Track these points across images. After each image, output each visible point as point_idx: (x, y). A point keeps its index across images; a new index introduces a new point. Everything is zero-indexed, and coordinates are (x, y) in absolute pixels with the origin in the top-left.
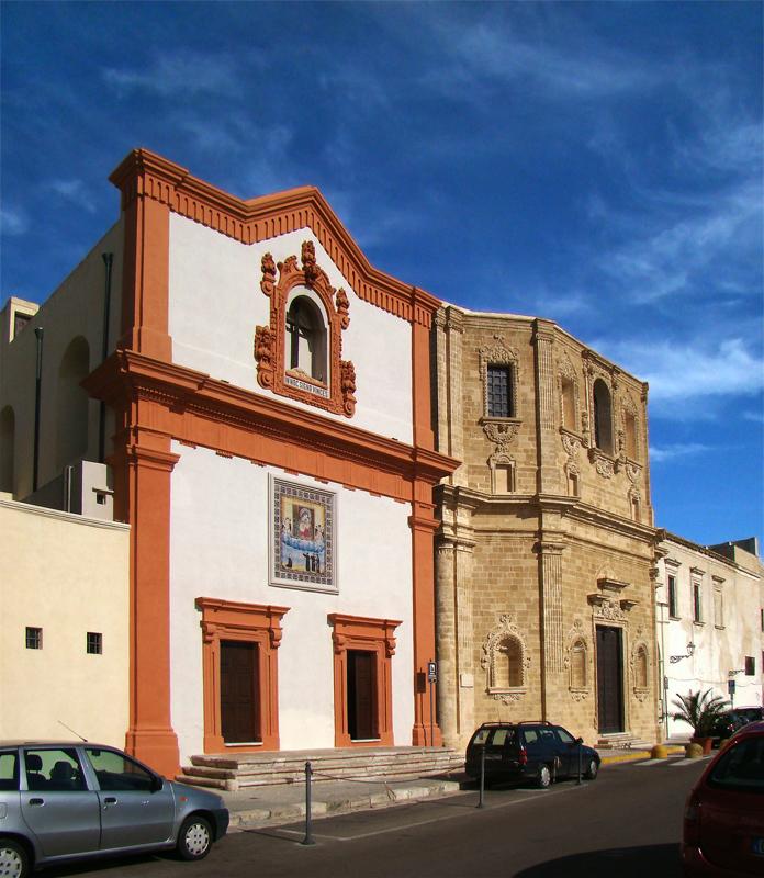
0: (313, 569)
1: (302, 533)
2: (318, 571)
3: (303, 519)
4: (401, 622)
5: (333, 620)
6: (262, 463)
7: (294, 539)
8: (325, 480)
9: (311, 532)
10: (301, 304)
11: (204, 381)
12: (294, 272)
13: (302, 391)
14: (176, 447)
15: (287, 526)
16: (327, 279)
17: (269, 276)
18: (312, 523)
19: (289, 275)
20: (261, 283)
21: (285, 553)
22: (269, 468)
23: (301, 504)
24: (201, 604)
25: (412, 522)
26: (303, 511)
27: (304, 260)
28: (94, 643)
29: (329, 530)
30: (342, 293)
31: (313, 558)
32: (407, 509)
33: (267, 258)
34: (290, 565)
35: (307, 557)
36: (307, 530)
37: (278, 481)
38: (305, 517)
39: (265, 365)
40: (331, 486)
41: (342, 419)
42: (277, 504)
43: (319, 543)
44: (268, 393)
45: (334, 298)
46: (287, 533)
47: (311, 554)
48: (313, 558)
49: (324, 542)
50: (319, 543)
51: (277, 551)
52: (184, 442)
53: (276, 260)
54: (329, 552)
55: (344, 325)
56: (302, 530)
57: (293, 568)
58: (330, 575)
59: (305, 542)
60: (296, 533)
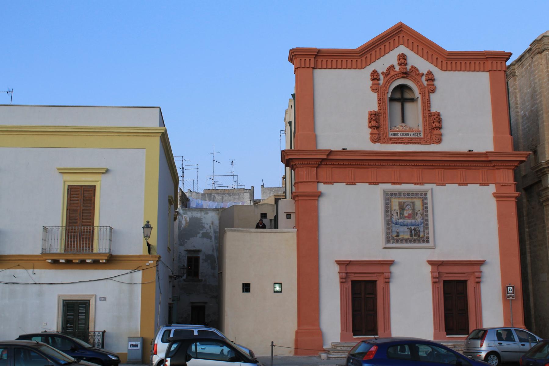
0: (415, 236)
1: (406, 217)
2: (419, 236)
3: (406, 209)
5: (431, 263)
6: (376, 183)
7: (400, 221)
8: (422, 184)
9: (413, 215)
10: (402, 88)
11: (331, 152)
12: (392, 73)
13: (403, 138)
14: (322, 187)
15: (395, 215)
16: (417, 69)
17: (376, 82)
18: (414, 209)
19: (389, 76)
20: (371, 87)
21: (394, 229)
24: (339, 263)
25: (497, 196)
26: (406, 204)
27: (400, 65)
28: (246, 288)
29: (427, 212)
30: (430, 73)
31: (415, 230)
32: (492, 188)
33: (375, 73)
34: (398, 236)
36: (409, 214)
37: (385, 191)
38: (408, 207)
39: (376, 131)
40: (427, 186)
43: (419, 219)
45: (424, 78)
46: (395, 218)
48: (415, 230)
49: (423, 219)
50: (419, 219)
52: (325, 183)
53: (380, 72)
54: (427, 225)
55: (433, 91)
56: (406, 214)
57: (400, 237)
58: (428, 237)
59: (408, 221)
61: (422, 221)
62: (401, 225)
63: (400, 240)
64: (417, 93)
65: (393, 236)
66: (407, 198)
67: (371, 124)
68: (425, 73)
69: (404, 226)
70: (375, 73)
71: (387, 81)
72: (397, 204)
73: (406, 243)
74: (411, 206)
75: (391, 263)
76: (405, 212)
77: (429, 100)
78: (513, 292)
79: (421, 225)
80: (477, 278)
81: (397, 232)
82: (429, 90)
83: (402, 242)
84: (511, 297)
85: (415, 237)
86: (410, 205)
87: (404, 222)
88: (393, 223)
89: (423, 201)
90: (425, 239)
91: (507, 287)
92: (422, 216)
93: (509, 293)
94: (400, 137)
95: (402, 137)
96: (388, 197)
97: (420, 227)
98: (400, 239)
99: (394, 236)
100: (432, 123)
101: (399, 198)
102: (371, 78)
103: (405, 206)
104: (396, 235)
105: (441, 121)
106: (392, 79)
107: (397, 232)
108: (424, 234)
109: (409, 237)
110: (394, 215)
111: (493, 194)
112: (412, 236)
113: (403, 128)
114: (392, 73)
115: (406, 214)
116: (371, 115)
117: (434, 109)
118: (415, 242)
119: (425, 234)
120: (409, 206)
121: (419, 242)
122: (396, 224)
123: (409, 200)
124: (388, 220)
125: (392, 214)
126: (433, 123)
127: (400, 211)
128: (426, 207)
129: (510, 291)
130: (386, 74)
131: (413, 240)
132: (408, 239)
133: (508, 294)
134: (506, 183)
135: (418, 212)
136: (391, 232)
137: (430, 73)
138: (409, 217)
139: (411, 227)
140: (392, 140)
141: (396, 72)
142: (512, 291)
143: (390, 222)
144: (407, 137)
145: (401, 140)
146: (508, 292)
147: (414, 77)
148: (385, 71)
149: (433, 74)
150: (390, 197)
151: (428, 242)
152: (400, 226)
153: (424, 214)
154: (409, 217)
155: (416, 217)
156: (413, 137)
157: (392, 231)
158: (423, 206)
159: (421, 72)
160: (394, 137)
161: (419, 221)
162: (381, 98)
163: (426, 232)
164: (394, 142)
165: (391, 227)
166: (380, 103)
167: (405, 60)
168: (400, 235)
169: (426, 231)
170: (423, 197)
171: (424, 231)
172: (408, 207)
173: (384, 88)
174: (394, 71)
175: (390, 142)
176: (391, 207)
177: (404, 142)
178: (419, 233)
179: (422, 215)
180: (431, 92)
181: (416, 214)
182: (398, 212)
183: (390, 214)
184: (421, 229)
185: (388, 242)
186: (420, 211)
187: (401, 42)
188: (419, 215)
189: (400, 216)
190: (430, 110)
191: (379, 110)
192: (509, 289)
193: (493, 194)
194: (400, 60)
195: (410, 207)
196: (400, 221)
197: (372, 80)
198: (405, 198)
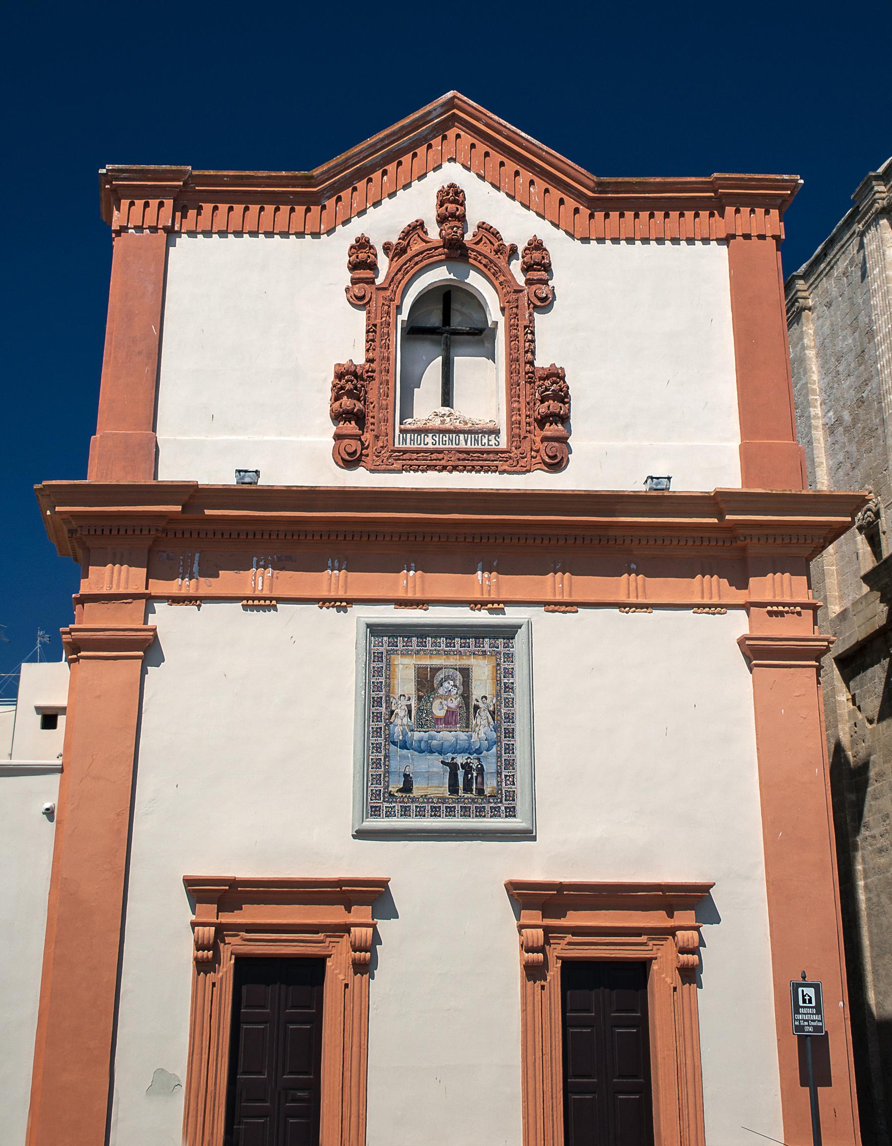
0: (468, 788)
1: (438, 720)
2: (481, 792)
3: (441, 691)
4: (714, 884)
7: (417, 735)
12: (417, 246)
13: (440, 452)
15: (401, 712)
16: (496, 234)
18: (466, 696)
19: (405, 257)
20: (347, 290)
21: (394, 765)
23: (437, 662)
26: (440, 675)
27: (442, 220)
29: (510, 703)
30: (536, 246)
31: (467, 767)
33: (362, 244)
34: (407, 787)
35: (453, 767)
36: (450, 712)
39: (351, 427)
46: (401, 723)
47: (460, 760)
48: (467, 767)
49: (496, 729)
53: (378, 243)
54: (510, 749)
55: (545, 304)
56: (439, 712)
57: (416, 793)
58: (511, 796)
59: (446, 736)
60: (424, 720)
61: (494, 735)
62: (421, 752)
63: (413, 806)
64: (495, 314)
65: (390, 789)
66: (447, 653)
67: (338, 403)
69: (431, 752)
70: (362, 244)
71: (399, 270)
72: (411, 674)
73: (435, 815)
74: (458, 683)
76: (437, 703)
77: (530, 328)
79: (488, 750)
80: (683, 951)
81: (406, 776)
83: (421, 813)
84: (811, 1029)
85: (466, 796)
86: (454, 680)
87: (432, 738)
88: (394, 743)
89: (498, 665)
90: (501, 802)
91: (796, 986)
92: (494, 720)
93: (801, 1010)
94: (430, 446)
95: (437, 446)
96: (381, 649)
98: (414, 800)
100: (538, 403)
101: (418, 652)
102: (350, 262)
105: (567, 395)
106: (416, 264)
107: (406, 776)
108: (498, 782)
109: (447, 794)
110: (397, 714)
111: (741, 642)
112: (458, 793)
113: (443, 422)
114: (417, 246)
116: (339, 376)
117: (542, 361)
119: (501, 782)
120: (452, 683)
121: (480, 813)
122: (404, 746)
123: (453, 661)
125: (392, 712)
126: (542, 402)
127: (419, 698)
128: (509, 688)
129: (804, 1001)
130: (395, 251)
131: (458, 807)
132: (443, 800)
133: (800, 1017)
134: (784, 605)
135: (481, 705)
136: (385, 777)
137: (536, 246)
138: (449, 720)
139: (453, 759)
140: (405, 457)
141: (427, 242)
142: (814, 1004)
143: (381, 740)
144: (454, 446)
145: (434, 456)
146: (797, 1008)
147: (486, 257)
148: (394, 240)
149: (545, 250)
150: (387, 651)
151: (511, 812)
152: (416, 753)
153: (500, 711)
154: (449, 720)
155: (474, 722)
156: (473, 446)
157: (387, 772)
158: (498, 682)
160: (412, 446)
161: (482, 735)
162: (378, 321)
163: (506, 776)
164: (410, 462)
165: (386, 756)
166: (373, 341)
167: (462, 204)
171: (499, 773)
172: (446, 684)
173: (388, 293)
174: (427, 242)
175: (397, 465)
176: (388, 685)
177: (443, 462)
178: (479, 779)
179: (492, 714)
181: (472, 710)
182: (413, 703)
184: (490, 767)
185: (375, 812)
186: (488, 701)
188: (484, 714)
189: (419, 718)
190: (531, 363)
191: (370, 361)
192: (803, 996)
193: (741, 642)
194: (445, 206)
195: (455, 686)
196: (417, 735)
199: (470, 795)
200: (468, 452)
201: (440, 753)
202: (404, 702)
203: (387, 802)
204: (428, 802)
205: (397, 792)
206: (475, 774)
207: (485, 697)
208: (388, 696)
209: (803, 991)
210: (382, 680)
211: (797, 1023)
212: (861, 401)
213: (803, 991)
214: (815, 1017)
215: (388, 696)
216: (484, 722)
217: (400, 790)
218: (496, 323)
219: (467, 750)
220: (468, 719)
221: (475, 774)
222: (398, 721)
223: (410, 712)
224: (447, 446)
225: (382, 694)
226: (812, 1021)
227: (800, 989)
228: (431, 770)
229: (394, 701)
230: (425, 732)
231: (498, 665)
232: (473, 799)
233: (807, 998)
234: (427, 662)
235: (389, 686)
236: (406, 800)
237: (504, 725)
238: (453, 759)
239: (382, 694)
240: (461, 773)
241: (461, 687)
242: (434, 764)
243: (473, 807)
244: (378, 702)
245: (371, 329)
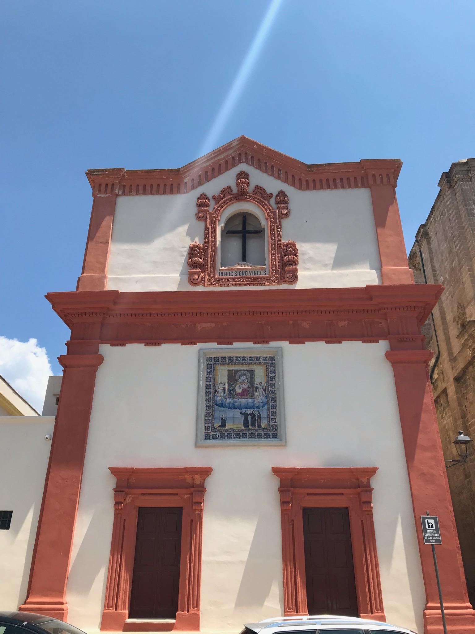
0: (253, 424)
1: (238, 394)
2: (260, 426)
3: (240, 381)
7: (228, 401)
9: (251, 390)
15: (220, 390)
18: (252, 382)
21: (217, 414)
22: (200, 345)
23: (237, 368)
29: (273, 385)
30: (282, 193)
31: (253, 415)
34: (223, 425)
35: (246, 416)
38: (243, 378)
41: (285, 287)
42: (208, 373)
43: (260, 397)
44: (200, 288)
45: (272, 201)
46: (220, 396)
49: (267, 397)
50: (260, 397)
51: (208, 414)
53: (210, 195)
54: (274, 406)
56: (238, 390)
57: (228, 426)
58: (275, 428)
59: (243, 401)
60: (231, 393)
61: (265, 400)
62: (230, 408)
64: (264, 223)
65: (215, 426)
66: (242, 364)
68: (275, 194)
69: (235, 408)
70: (203, 196)
72: (225, 373)
73: (237, 438)
74: (248, 377)
75: (206, 472)
76: (237, 386)
78: (437, 529)
79: (263, 407)
81: (223, 420)
82: (280, 215)
84: (434, 541)
85: (252, 428)
86: (246, 376)
87: (235, 402)
88: (217, 405)
90: (270, 431)
92: (265, 393)
94: (234, 276)
96: (211, 363)
97: (262, 410)
98: (226, 431)
99: (216, 425)
101: (228, 364)
103: (237, 377)
104: (220, 424)
107: (223, 420)
108: (268, 422)
109: (243, 428)
110: (218, 391)
112: (248, 427)
115: (238, 390)
118: (252, 436)
119: (270, 421)
120: (245, 377)
122: (222, 405)
123: (245, 367)
124: (208, 400)
127: (229, 384)
129: (429, 526)
132: (241, 430)
133: (427, 535)
135: (259, 386)
136: (212, 420)
137: (282, 193)
138: (244, 393)
139: (246, 411)
142: (434, 528)
143: (211, 403)
146: (425, 530)
148: (217, 194)
150: (214, 364)
154: (244, 393)
155: (256, 394)
157: (213, 418)
158: (267, 376)
159: (269, 191)
161: (260, 400)
163: (272, 419)
168: (227, 424)
169: (271, 417)
170: (268, 363)
171: (268, 418)
172: (242, 378)
176: (214, 379)
178: (259, 420)
179: (265, 390)
180: (283, 216)
182: (226, 386)
183: (212, 390)
184: (264, 414)
185: (207, 437)
187: (244, 159)
188: (261, 391)
189: (229, 393)
192: (428, 524)
195: (246, 378)
196: (228, 401)
197: (198, 207)
198: (238, 364)
199: (254, 428)
200: (251, 278)
201: (240, 409)
202: (222, 386)
203: (213, 432)
204: (233, 432)
205: (219, 427)
206: (256, 418)
207: (261, 383)
208: (214, 384)
209: (428, 521)
210: (211, 376)
211: (426, 538)
212: (452, 269)
213: (428, 521)
214: (436, 535)
215: (214, 384)
216: (261, 394)
217: (219, 426)
218: (264, 225)
219: (253, 407)
220: (253, 392)
221: (256, 418)
222: (219, 395)
223: (224, 390)
224: (241, 276)
225: (211, 383)
226: (435, 537)
227: (426, 520)
228: (235, 416)
229: (217, 386)
230: (232, 399)
231: (267, 368)
232: (256, 430)
233: (430, 525)
234: (232, 368)
235: (215, 379)
236: (222, 431)
237: (271, 396)
238: (246, 411)
239: (211, 383)
240: (250, 417)
241: (249, 379)
242: (237, 413)
243: (256, 433)
244: (208, 386)
245: (207, 229)
